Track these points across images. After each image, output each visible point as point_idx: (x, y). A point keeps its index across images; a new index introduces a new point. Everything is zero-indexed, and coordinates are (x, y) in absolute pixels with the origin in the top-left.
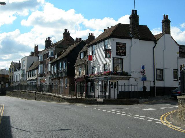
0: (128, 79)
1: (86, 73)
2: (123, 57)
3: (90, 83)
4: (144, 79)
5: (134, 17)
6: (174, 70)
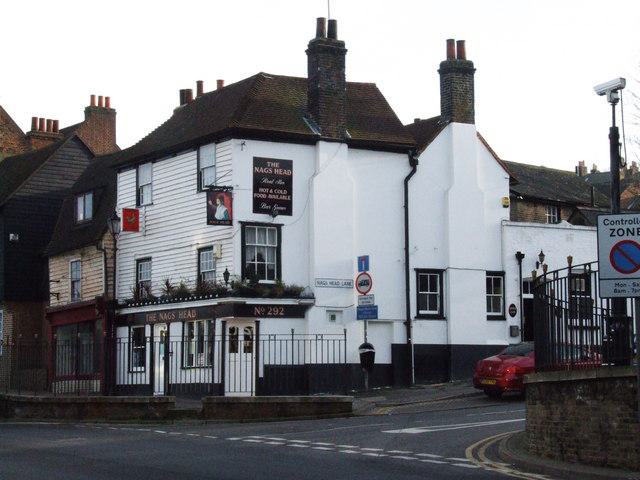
0: (299, 312)
1: (107, 286)
2: (280, 219)
3: (124, 333)
4: (368, 313)
5: (327, 49)
6: (489, 273)
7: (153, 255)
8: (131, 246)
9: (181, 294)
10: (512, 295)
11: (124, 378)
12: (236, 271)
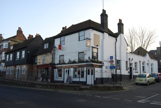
0: (101, 67)
3: (56, 71)
5: (104, 16)
6: (126, 62)
7: (65, 55)
8: (58, 53)
9: (74, 62)
10: (129, 66)
11: (56, 79)
12: (91, 57)
